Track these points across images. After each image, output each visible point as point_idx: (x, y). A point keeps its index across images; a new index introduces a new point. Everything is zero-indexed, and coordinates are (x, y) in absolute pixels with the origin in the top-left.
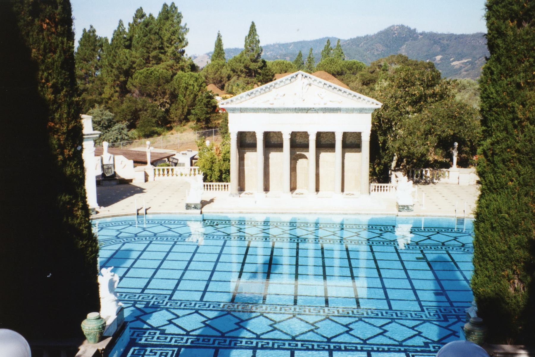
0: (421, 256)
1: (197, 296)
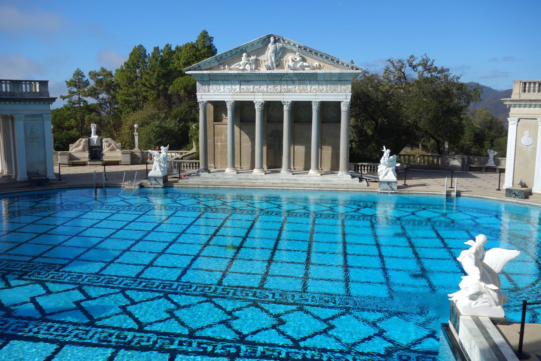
0: (400, 231)
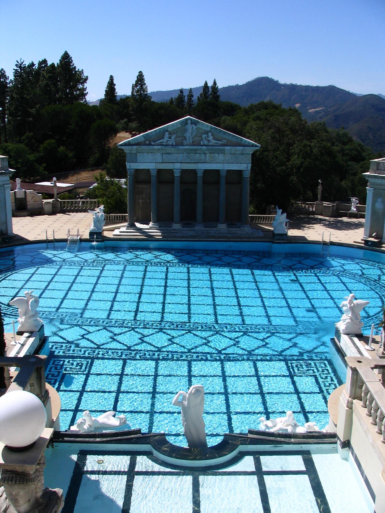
1: (104, 315)
